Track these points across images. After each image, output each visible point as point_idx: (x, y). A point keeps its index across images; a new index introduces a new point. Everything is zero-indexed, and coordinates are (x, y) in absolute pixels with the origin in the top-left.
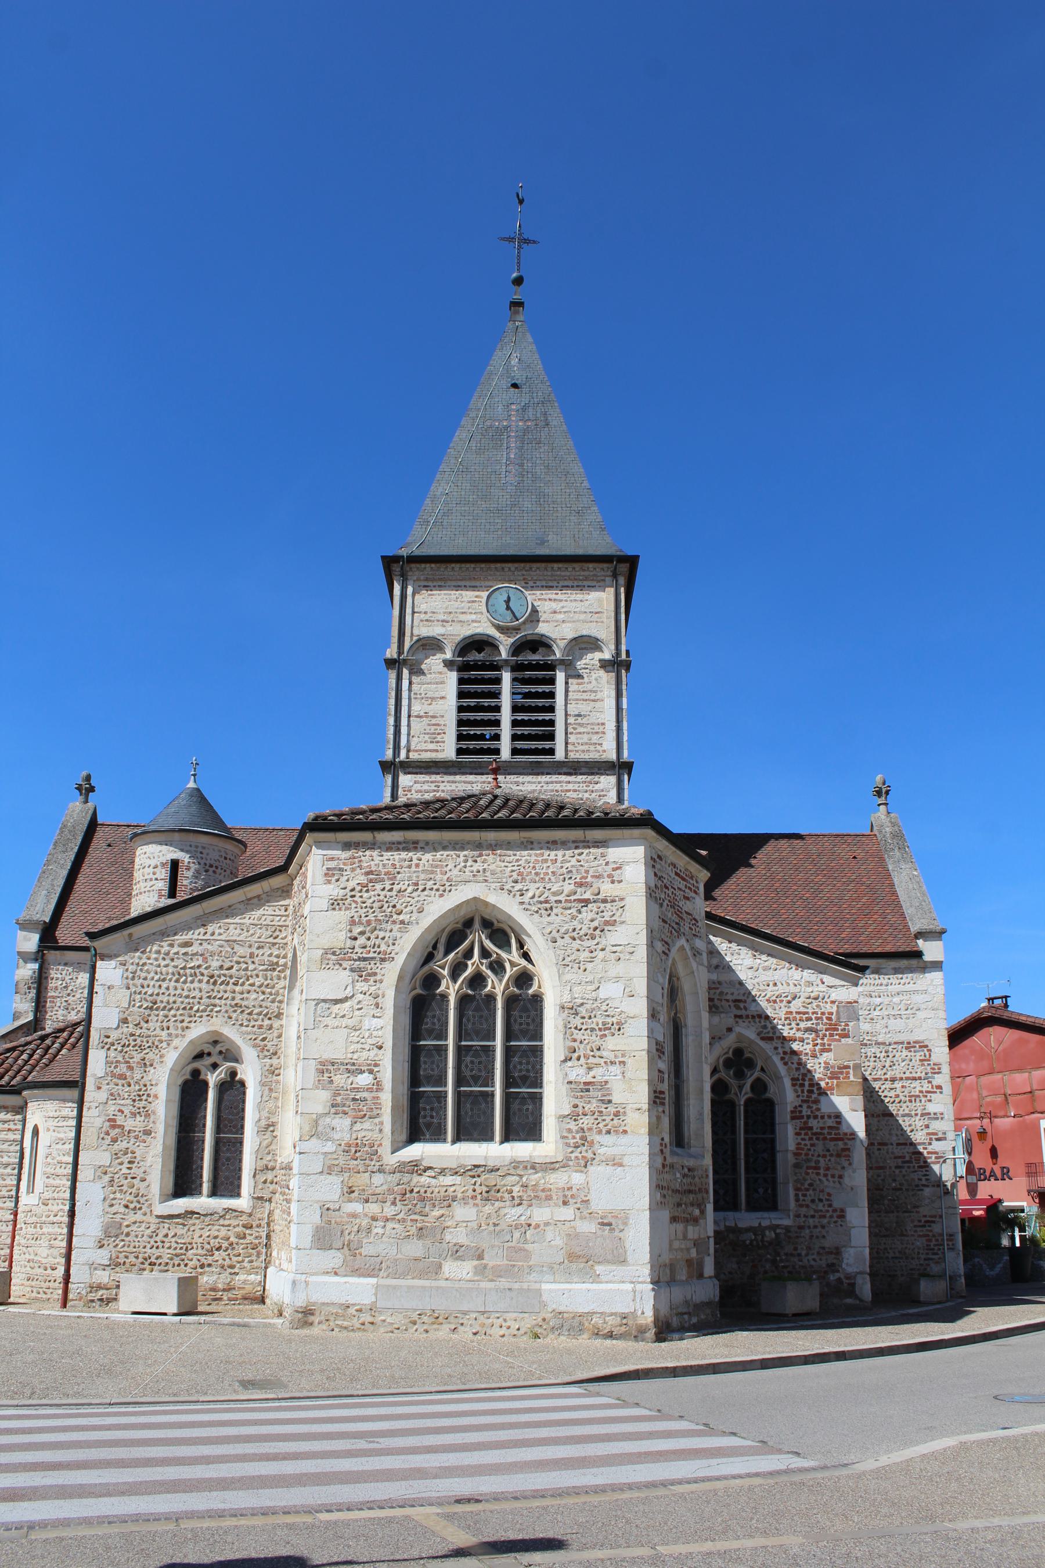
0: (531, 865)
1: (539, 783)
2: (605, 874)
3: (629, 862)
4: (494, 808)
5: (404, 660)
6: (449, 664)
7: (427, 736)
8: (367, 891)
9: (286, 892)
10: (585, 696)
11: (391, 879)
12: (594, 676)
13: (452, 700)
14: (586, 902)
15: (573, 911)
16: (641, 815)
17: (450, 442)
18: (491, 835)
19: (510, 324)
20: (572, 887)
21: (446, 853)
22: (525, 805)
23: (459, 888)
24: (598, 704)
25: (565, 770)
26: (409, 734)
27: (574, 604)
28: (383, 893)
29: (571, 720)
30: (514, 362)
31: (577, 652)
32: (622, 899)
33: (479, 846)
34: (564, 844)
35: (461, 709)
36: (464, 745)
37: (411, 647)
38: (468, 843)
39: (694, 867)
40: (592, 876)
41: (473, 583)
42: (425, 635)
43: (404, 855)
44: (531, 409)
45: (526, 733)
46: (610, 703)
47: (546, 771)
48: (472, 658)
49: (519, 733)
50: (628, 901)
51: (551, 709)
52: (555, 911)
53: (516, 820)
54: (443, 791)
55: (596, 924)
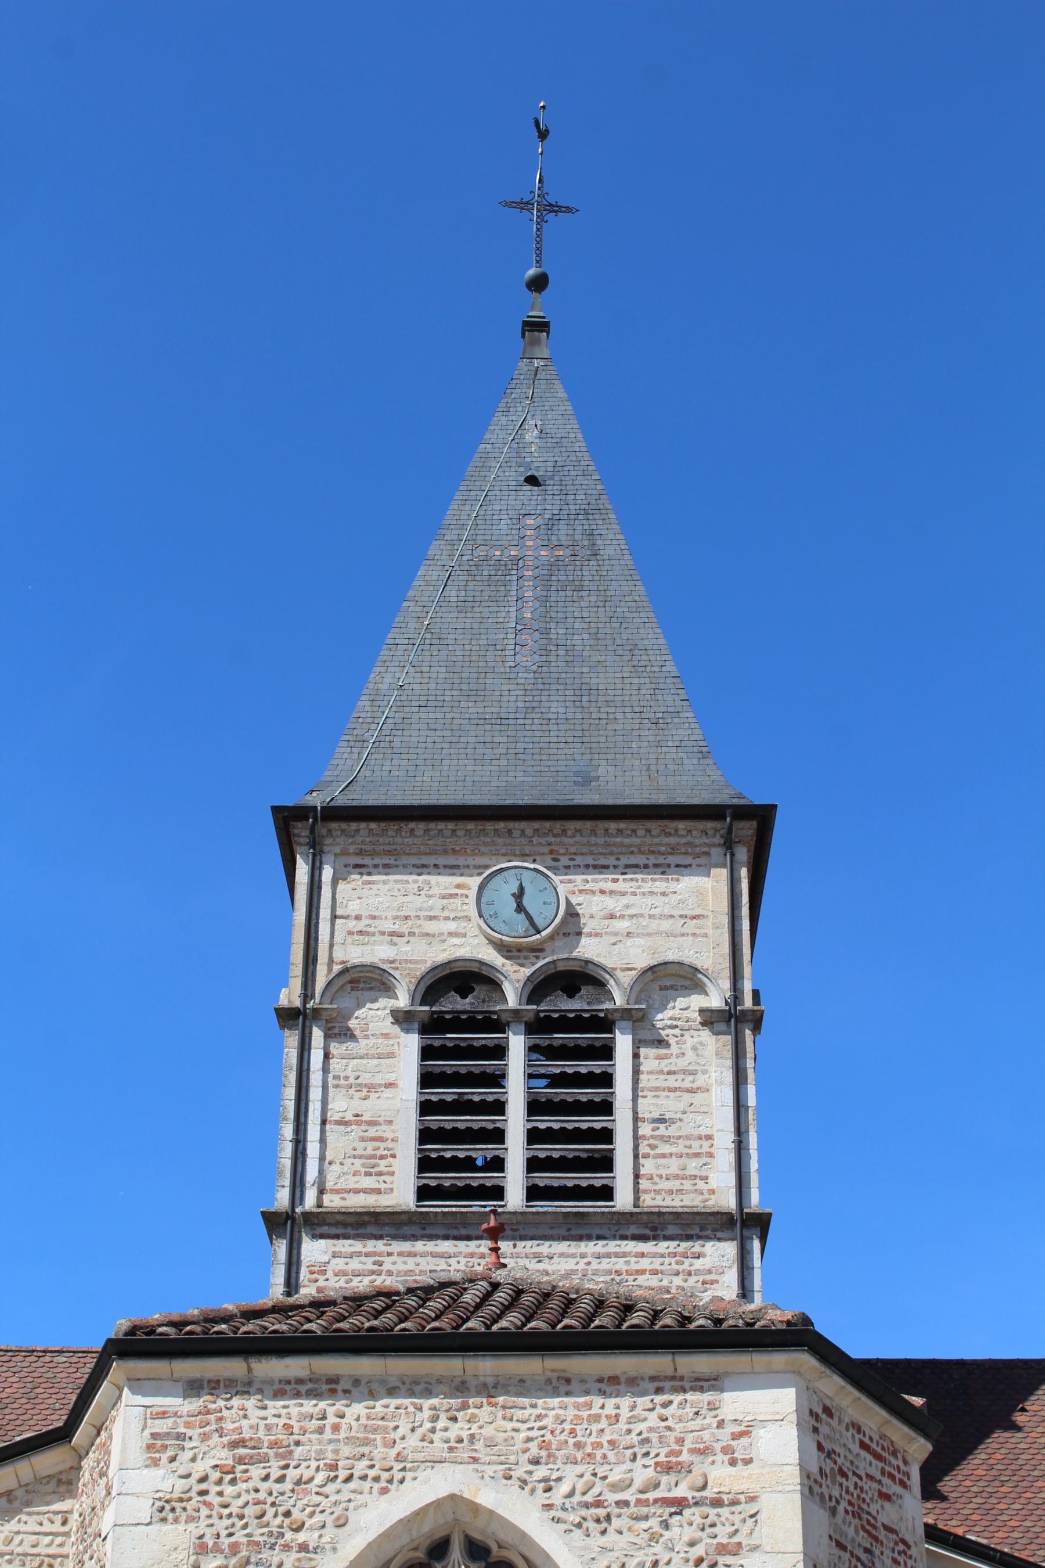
0: (567, 1426)
1: (583, 1256)
2: (718, 1447)
3: (766, 1418)
4: (491, 1309)
5: (315, 1011)
6: (402, 1019)
7: (358, 1162)
8: (233, 1482)
9: (65, 1483)
10: (672, 1082)
11: (282, 1456)
12: (689, 1041)
13: (408, 1091)
14: (680, 1504)
15: (654, 1523)
16: (789, 1323)
17: (409, 586)
18: (485, 1366)
19: (523, 365)
20: (650, 1473)
21: (394, 1402)
22: (554, 1303)
23: (422, 1475)
24: (698, 1098)
25: (633, 1230)
26: (322, 1158)
27: (649, 900)
28: (264, 1486)
29: (645, 1129)
30: (531, 435)
31: (656, 996)
32: (752, 1499)
33: (461, 1388)
34: (632, 1384)
35: (426, 1108)
36: (433, 1179)
37: (329, 984)
38: (439, 1381)
39: (899, 1432)
40: (692, 1451)
41: (451, 860)
42: (356, 961)
43: (309, 1406)
44: (562, 525)
45: (556, 1155)
46: (722, 1095)
47: (596, 1231)
48: (448, 1007)
49: (542, 1155)
50: (766, 1503)
51: (606, 1108)
52: (616, 1523)
53: (536, 1334)
54: (390, 1273)
55: (699, 1551)
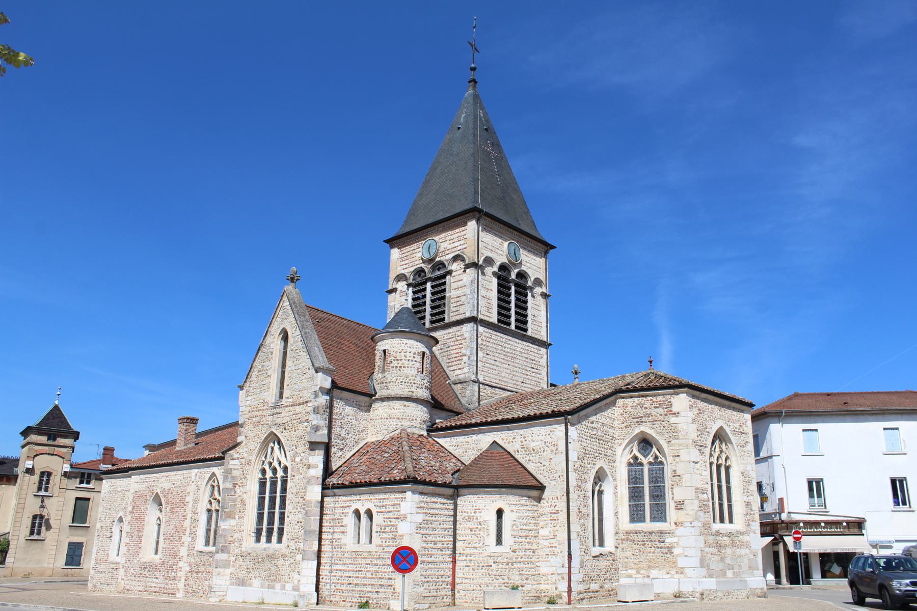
6: (494, 274)
